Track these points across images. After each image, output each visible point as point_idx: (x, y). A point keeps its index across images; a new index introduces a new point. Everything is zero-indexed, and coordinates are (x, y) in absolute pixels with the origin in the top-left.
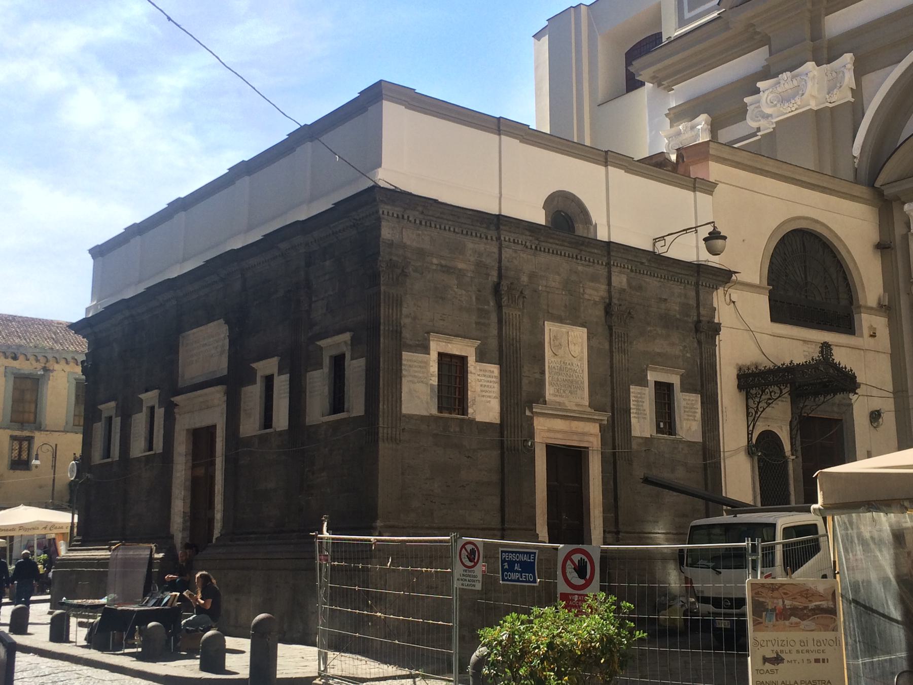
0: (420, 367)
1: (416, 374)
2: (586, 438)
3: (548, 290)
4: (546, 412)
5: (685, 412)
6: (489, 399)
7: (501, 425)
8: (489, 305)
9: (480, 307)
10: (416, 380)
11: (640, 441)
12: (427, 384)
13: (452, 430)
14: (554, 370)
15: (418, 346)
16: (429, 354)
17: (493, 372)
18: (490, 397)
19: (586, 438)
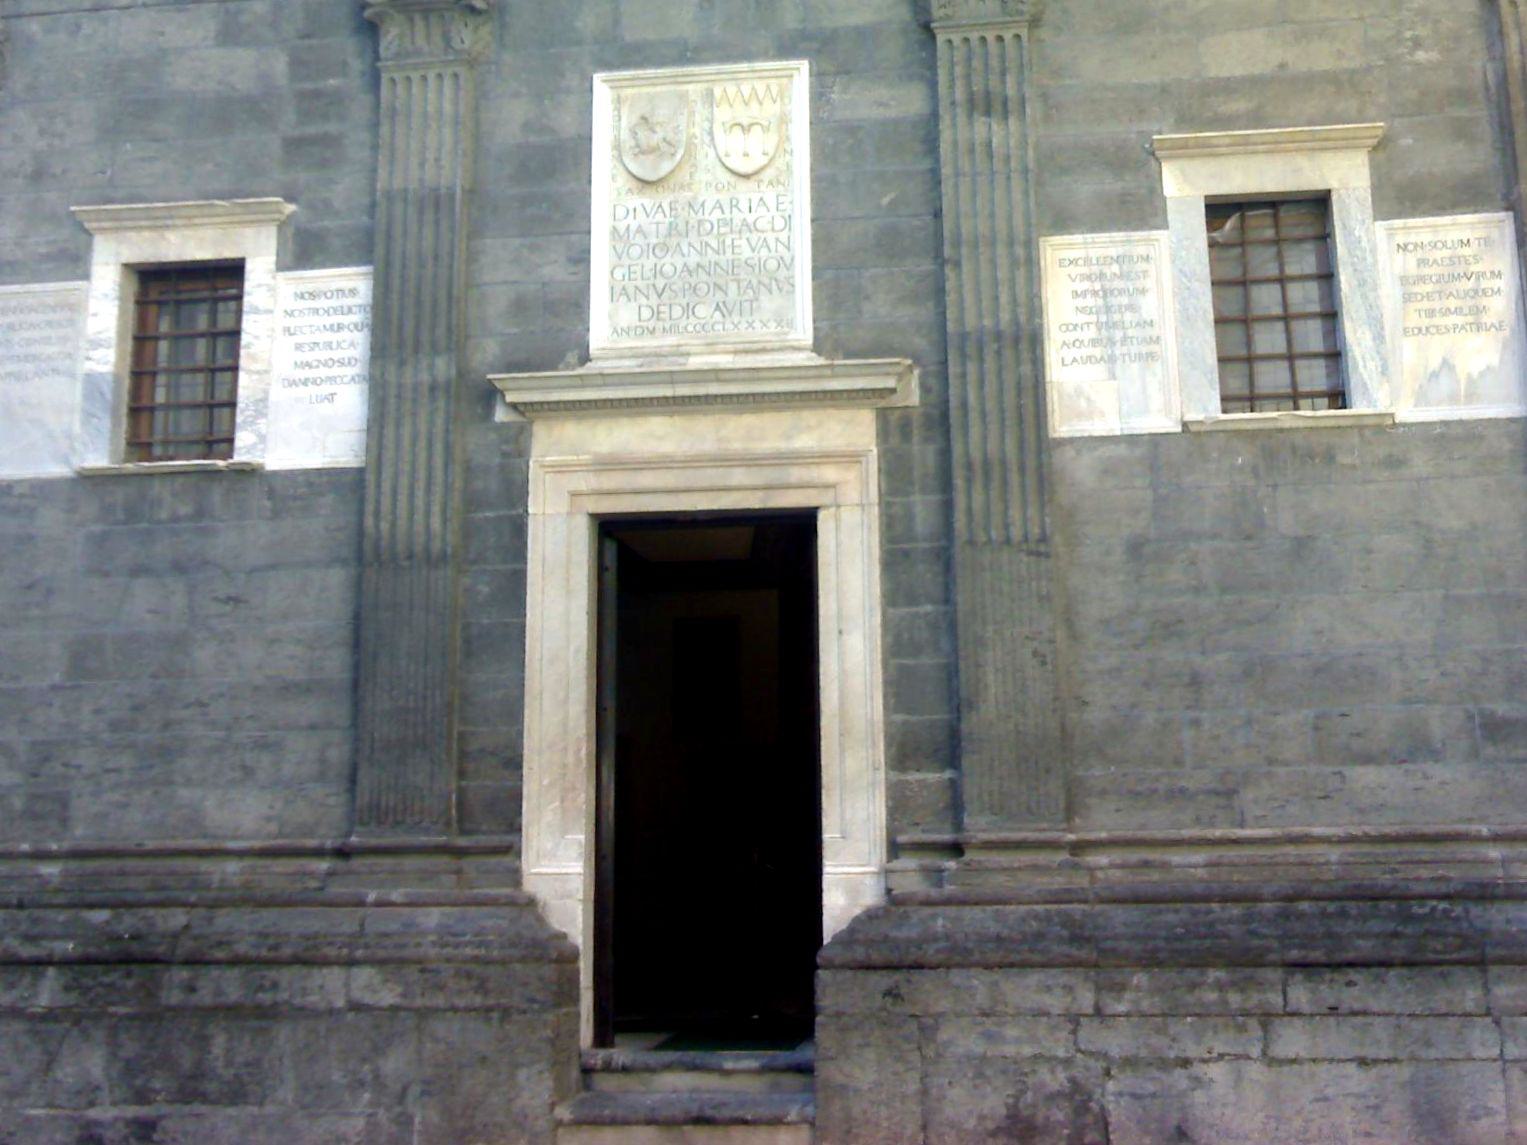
1: (35, 349)
2: (796, 474)
4: (555, 396)
5: (1407, 298)
6: (326, 389)
9: (309, 86)
10: (29, 367)
11: (1122, 450)
12: (72, 375)
14: (639, 239)
15: (47, 257)
16: (86, 276)
17: (353, 292)
18: (331, 379)
19: (796, 474)
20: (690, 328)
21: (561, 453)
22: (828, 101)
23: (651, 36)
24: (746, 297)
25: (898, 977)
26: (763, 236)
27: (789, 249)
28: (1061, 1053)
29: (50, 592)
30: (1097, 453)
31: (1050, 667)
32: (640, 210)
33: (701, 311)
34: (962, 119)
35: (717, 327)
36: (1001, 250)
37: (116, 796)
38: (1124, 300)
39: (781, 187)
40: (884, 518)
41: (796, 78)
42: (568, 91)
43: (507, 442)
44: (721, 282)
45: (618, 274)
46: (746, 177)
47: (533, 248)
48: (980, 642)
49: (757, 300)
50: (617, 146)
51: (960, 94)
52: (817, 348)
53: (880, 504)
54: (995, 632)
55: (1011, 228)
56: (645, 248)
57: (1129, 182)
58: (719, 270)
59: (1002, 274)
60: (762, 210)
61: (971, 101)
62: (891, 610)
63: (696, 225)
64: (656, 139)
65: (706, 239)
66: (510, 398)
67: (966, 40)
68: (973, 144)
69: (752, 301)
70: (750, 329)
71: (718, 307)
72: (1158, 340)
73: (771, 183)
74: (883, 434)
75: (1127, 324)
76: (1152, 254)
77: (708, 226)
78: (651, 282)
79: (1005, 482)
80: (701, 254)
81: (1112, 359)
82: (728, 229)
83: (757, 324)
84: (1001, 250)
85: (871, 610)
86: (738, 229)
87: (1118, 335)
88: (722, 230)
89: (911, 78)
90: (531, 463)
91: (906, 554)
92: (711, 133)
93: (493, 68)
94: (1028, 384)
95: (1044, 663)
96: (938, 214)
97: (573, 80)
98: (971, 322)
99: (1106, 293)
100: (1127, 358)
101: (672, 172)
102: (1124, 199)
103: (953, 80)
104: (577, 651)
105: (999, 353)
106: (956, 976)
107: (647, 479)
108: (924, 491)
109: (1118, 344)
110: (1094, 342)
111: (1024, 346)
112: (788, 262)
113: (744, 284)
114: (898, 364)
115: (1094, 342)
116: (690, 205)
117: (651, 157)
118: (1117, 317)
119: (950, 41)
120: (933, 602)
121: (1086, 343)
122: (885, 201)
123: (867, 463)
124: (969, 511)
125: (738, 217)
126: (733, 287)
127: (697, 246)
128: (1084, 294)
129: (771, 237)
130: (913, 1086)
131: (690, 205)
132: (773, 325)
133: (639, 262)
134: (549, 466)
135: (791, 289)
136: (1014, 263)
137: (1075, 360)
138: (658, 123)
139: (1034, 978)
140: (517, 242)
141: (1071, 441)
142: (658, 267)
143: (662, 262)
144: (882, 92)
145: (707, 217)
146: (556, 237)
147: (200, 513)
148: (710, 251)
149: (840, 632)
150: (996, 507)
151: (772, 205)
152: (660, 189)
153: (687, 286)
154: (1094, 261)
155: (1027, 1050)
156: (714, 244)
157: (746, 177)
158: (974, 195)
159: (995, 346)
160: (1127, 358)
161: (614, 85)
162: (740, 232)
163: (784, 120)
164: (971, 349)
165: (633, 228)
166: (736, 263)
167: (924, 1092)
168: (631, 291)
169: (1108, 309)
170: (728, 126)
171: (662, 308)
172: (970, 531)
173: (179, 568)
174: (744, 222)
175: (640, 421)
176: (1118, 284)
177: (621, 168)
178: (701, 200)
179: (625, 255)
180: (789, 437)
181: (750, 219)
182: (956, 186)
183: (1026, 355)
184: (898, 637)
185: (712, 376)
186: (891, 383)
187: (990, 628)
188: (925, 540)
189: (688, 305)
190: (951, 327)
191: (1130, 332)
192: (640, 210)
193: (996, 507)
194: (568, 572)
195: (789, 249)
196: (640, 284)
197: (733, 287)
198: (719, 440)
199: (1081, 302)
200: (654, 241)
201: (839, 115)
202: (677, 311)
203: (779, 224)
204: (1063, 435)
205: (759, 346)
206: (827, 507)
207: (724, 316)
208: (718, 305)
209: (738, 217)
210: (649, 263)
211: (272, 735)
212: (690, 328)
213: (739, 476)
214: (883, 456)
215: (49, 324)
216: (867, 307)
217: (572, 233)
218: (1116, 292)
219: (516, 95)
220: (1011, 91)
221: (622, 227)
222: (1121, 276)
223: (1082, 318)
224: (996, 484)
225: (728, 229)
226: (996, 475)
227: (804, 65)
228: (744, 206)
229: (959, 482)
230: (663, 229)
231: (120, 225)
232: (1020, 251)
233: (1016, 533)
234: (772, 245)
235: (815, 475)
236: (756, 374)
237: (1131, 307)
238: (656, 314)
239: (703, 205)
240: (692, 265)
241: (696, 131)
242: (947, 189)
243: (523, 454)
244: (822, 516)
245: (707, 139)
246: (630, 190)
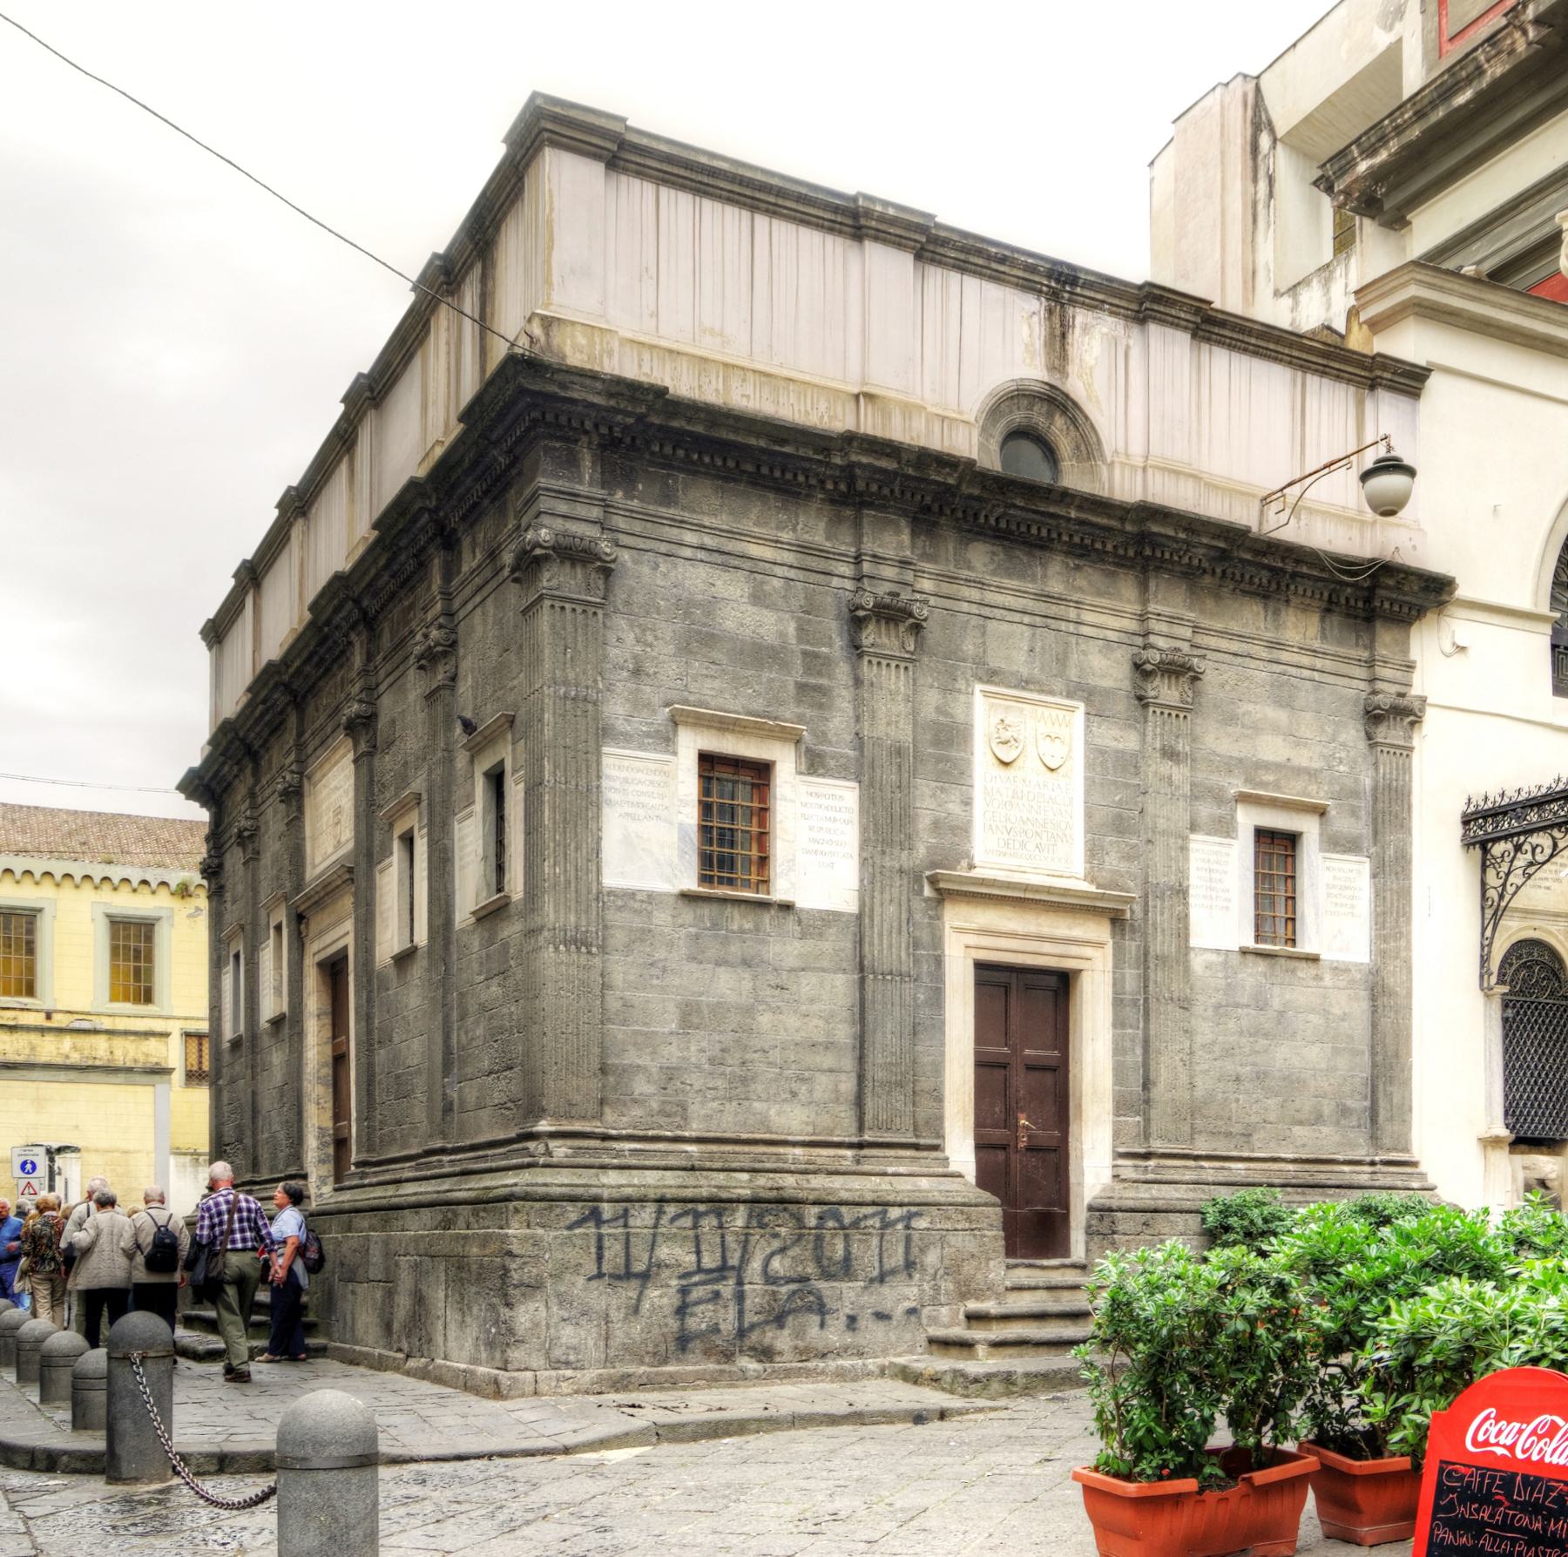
0: (652, 782)
1: (642, 799)
3: (986, 611)
7: (859, 917)
8: (831, 646)
9: (808, 648)
10: (641, 812)
13: (735, 927)
15: (648, 735)
16: (675, 753)
29: (664, 970)
37: (715, 1105)
42: (959, 691)
147: (757, 929)
161: (986, 694)
173: (746, 963)
211: (807, 1074)
215: (652, 782)
219: (932, 687)
231: (701, 722)
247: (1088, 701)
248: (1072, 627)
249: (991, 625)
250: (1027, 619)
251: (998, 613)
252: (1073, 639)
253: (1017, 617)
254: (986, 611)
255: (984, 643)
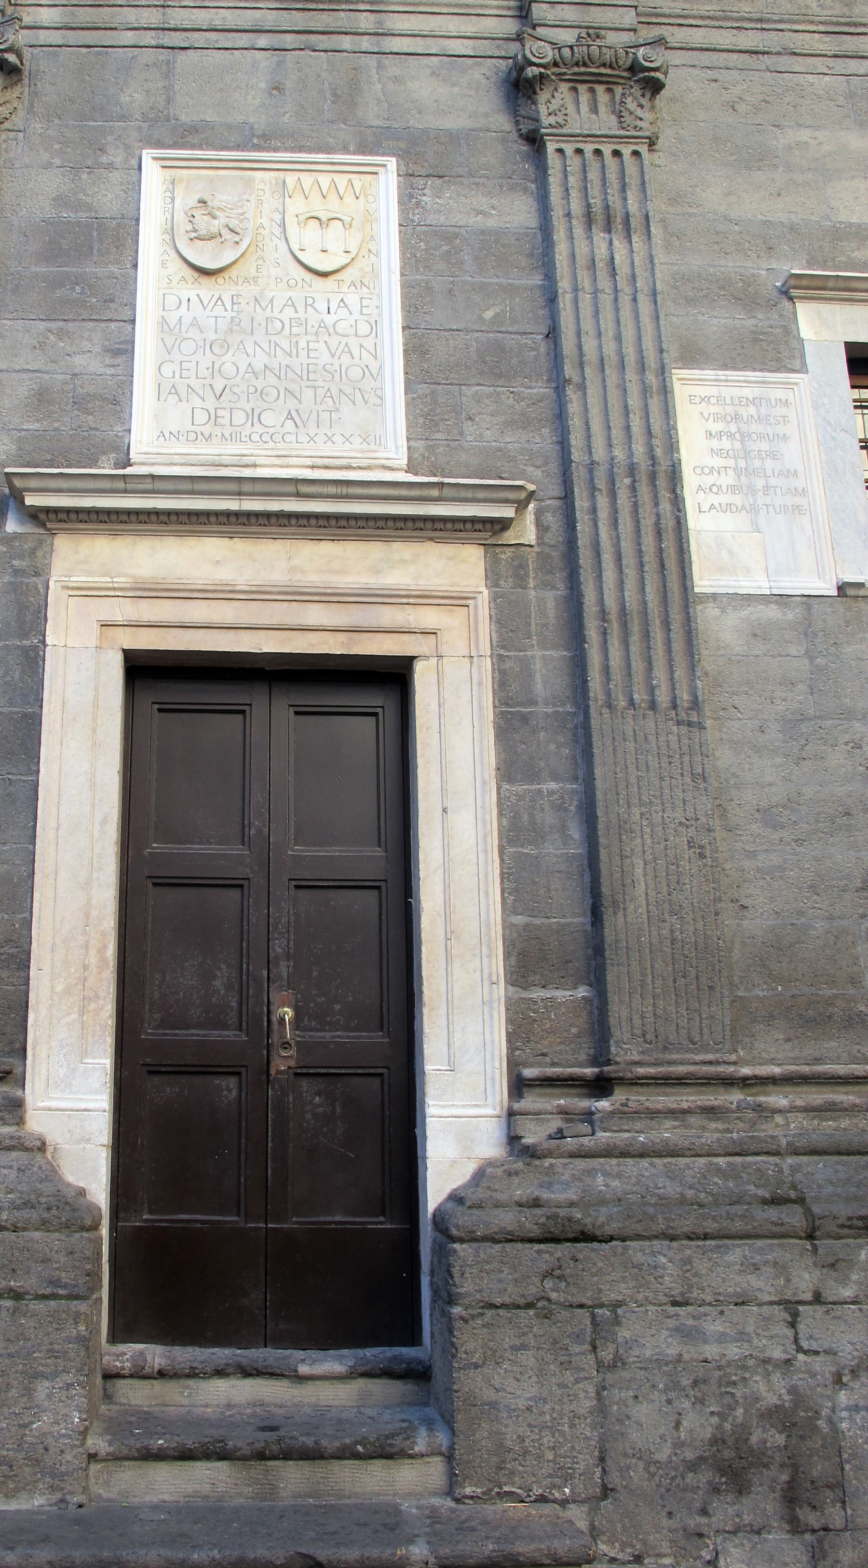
3: (176, 39)
11: (773, 612)
14: (194, 333)
20: (255, 437)
21: (89, 573)
22: (418, 204)
23: (210, 116)
24: (324, 407)
25: (562, 1250)
26: (344, 340)
27: (376, 357)
28: (777, 1354)
30: (745, 613)
31: (709, 861)
32: (194, 299)
33: (268, 418)
34: (579, 231)
35: (289, 438)
36: (631, 375)
38: (765, 446)
39: (365, 290)
40: (497, 675)
41: (382, 177)
42: (110, 167)
43: (21, 557)
44: (293, 387)
45: (167, 370)
46: (324, 275)
47: (61, 334)
48: (622, 827)
49: (337, 410)
50: (171, 231)
51: (576, 207)
52: (411, 468)
53: (491, 656)
54: (642, 815)
55: (640, 351)
56: (201, 343)
57: (760, 320)
58: (290, 374)
59: (634, 401)
60: (343, 312)
61: (589, 218)
62: (506, 786)
63: (264, 323)
64: (215, 225)
65: (274, 338)
66: (30, 500)
67: (579, 151)
68: (593, 260)
69: (331, 412)
70: (329, 443)
71: (290, 416)
72: (804, 492)
73: (353, 284)
74: (493, 577)
75: (769, 472)
76: (791, 400)
77: (278, 325)
78: (209, 381)
79: (646, 635)
80: (269, 354)
81: (754, 510)
82: (301, 330)
83: (338, 438)
84: (631, 375)
85: (484, 782)
86: (314, 330)
87: (760, 483)
88: (295, 330)
89: (512, 188)
90: (51, 584)
91: (524, 719)
92: (283, 226)
93: (21, 135)
94: (668, 523)
95: (702, 856)
96: (553, 334)
97: (115, 156)
98: (600, 453)
99: (744, 437)
100: (771, 509)
101: (234, 263)
102: (756, 337)
103: (567, 190)
104: (104, 821)
105: (633, 489)
106: (636, 1250)
107: (198, 612)
108: (543, 645)
109: (761, 493)
110: (733, 489)
111: (662, 483)
112: (375, 372)
113: (321, 392)
114: (521, 488)
115: (733, 489)
116: (256, 299)
117: (209, 243)
118: (757, 463)
119: (560, 151)
120: (555, 777)
121: (724, 489)
122: (488, 315)
123: (476, 607)
124: (606, 670)
125: (314, 319)
126: (308, 394)
127: (265, 346)
128: (720, 434)
129: (353, 342)
130: (587, 1404)
131: (256, 299)
132: (357, 440)
133: (194, 359)
134: (73, 589)
135: (379, 401)
136: (645, 391)
137: (712, 507)
138: (219, 209)
139: (737, 1253)
140: (42, 326)
141: (714, 596)
142: (217, 367)
143: (223, 359)
144: (482, 201)
145: (276, 314)
146: (91, 324)
148: (279, 352)
149: (445, 810)
150: (638, 666)
151: (356, 309)
152: (220, 280)
153: (252, 390)
154: (728, 401)
155: (734, 1351)
156: (285, 345)
157: (324, 275)
158: (597, 313)
159: (627, 481)
160: (771, 509)
161: (166, 164)
162: (316, 334)
163: (370, 218)
164: (601, 483)
165: (186, 320)
166: (311, 368)
167: (601, 1409)
168: (183, 390)
169: (747, 455)
170: (302, 218)
171: (220, 413)
172: (608, 693)
174: (322, 324)
175: (192, 541)
176: (755, 427)
177: (174, 255)
178: (271, 294)
179: (176, 349)
180: (376, 571)
181: (330, 320)
182: (576, 301)
183: (665, 495)
184: (516, 817)
185: (291, 489)
186: (508, 512)
187: (636, 811)
188: (547, 704)
189: (253, 410)
190: (576, 455)
191: (773, 482)
192: (194, 299)
193: (638, 666)
194: (94, 720)
195: (376, 357)
196: (193, 382)
197: (308, 394)
198: (292, 569)
199: (715, 444)
200: (212, 336)
201: (431, 219)
202: (239, 418)
203: (364, 328)
204: (704, 590)
205: (344, 462)
206: (427, 658)
207: (297, 426)
208: (289, 412)
209: (314, 319)
210: (206, 360)
212: (255, 437)
213: (316, 615)
214: (494, 598)
216: (469, 428)
217: (111, 320)
218: (754, 436)
219: (47, 166)
220: (633, 206)
221: (173, 322)
222: (759, 419)
223: (717, 462)
224: (635, 638)
225: (301, 330)
226: (635, 628)
227: (392, 163)
228: (322, 306)
229: (592, 633)
230: (223, 325)
232: (651, 379)
233: (663, 697)
234: (356, 353)
235: (411, 618)
236: (345, 490)
237: (773, 455)
238: (214, 418)
239: (272, 301)
240: (258, 366)
241: (265, 221)
242: (565, 302)
243: (41, 572)
244: (419, 668)
245: (278, 231)
246: (183, 279)
247: (403, 156)
248: (365, 43)
249: (183, 58)
250: (263, 41)
251: (198, 39)
252: (371, 62)
253: (243, 40)
254: (176, 39)
255: (168, 88)
